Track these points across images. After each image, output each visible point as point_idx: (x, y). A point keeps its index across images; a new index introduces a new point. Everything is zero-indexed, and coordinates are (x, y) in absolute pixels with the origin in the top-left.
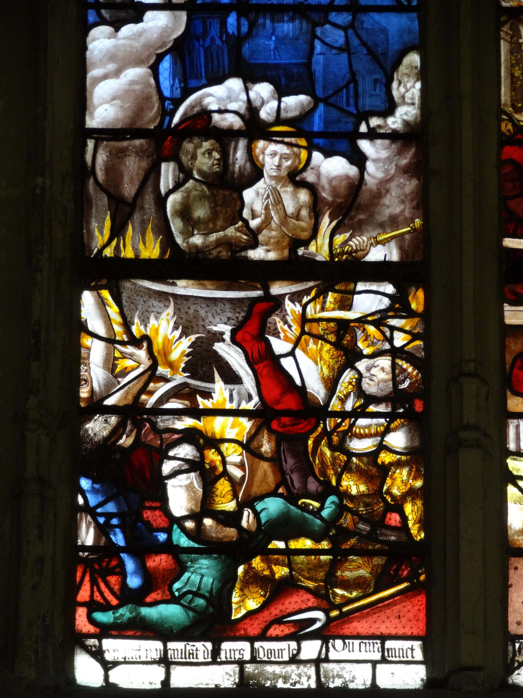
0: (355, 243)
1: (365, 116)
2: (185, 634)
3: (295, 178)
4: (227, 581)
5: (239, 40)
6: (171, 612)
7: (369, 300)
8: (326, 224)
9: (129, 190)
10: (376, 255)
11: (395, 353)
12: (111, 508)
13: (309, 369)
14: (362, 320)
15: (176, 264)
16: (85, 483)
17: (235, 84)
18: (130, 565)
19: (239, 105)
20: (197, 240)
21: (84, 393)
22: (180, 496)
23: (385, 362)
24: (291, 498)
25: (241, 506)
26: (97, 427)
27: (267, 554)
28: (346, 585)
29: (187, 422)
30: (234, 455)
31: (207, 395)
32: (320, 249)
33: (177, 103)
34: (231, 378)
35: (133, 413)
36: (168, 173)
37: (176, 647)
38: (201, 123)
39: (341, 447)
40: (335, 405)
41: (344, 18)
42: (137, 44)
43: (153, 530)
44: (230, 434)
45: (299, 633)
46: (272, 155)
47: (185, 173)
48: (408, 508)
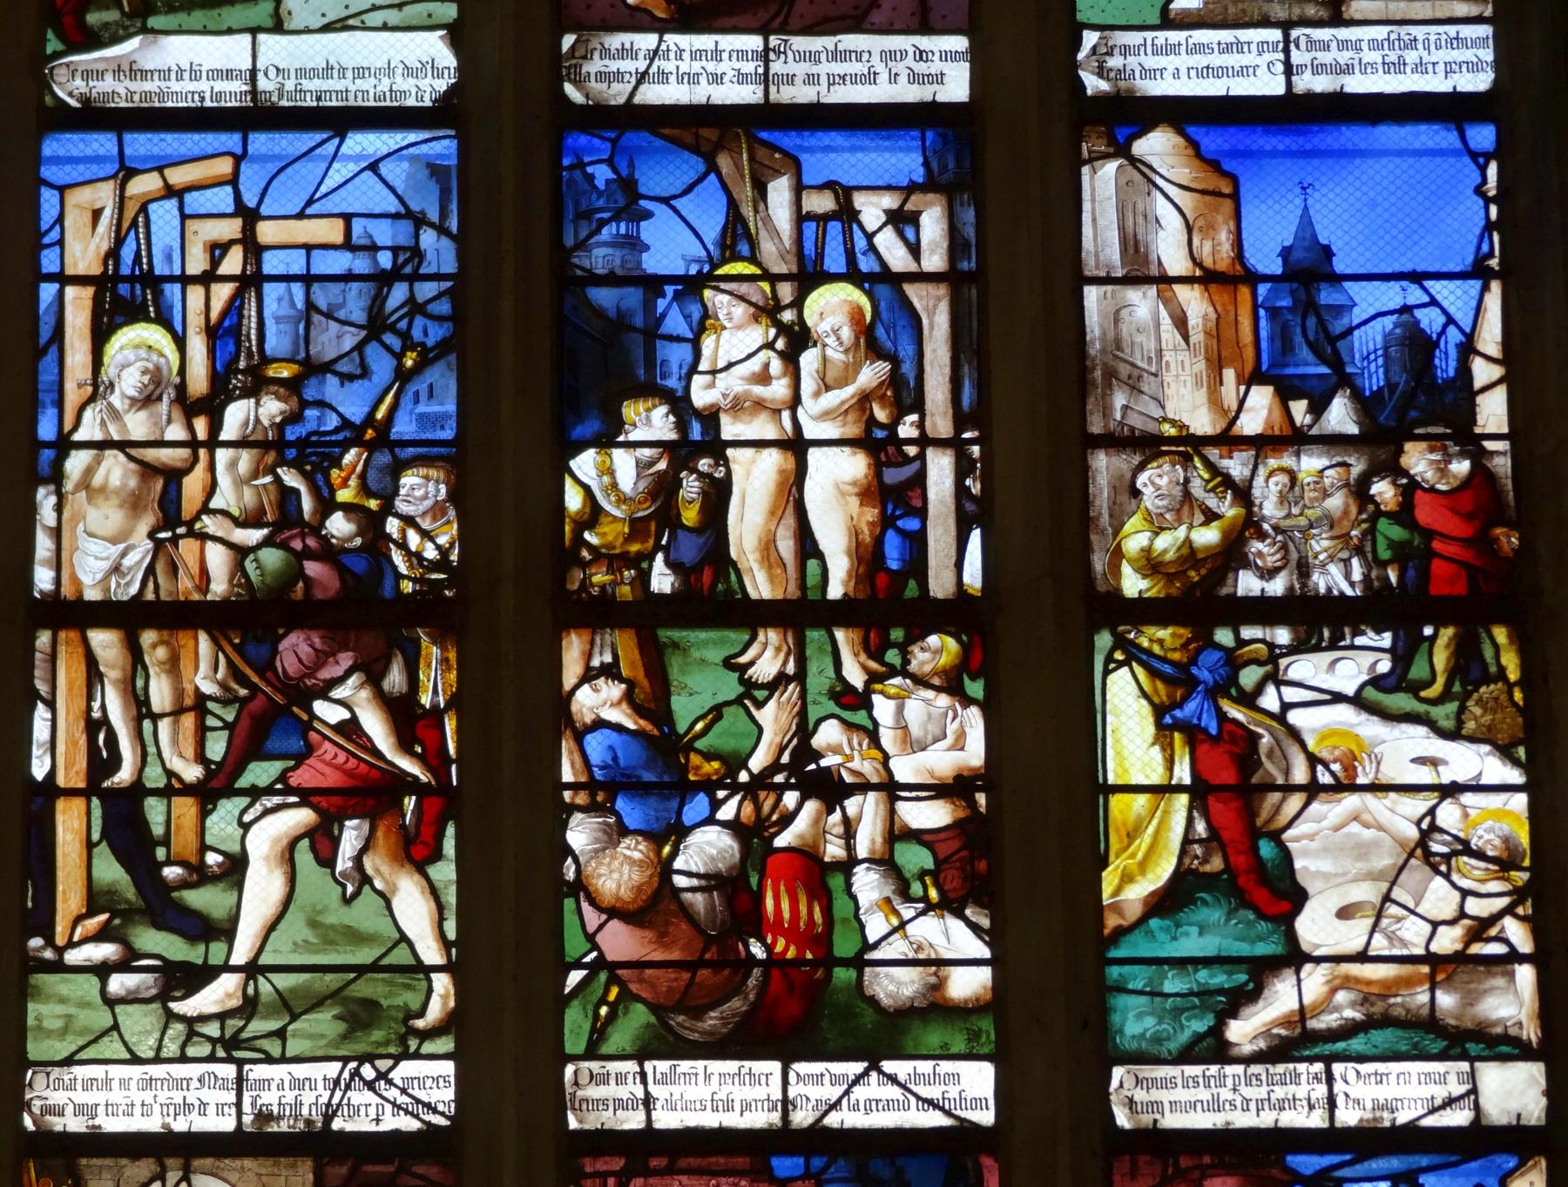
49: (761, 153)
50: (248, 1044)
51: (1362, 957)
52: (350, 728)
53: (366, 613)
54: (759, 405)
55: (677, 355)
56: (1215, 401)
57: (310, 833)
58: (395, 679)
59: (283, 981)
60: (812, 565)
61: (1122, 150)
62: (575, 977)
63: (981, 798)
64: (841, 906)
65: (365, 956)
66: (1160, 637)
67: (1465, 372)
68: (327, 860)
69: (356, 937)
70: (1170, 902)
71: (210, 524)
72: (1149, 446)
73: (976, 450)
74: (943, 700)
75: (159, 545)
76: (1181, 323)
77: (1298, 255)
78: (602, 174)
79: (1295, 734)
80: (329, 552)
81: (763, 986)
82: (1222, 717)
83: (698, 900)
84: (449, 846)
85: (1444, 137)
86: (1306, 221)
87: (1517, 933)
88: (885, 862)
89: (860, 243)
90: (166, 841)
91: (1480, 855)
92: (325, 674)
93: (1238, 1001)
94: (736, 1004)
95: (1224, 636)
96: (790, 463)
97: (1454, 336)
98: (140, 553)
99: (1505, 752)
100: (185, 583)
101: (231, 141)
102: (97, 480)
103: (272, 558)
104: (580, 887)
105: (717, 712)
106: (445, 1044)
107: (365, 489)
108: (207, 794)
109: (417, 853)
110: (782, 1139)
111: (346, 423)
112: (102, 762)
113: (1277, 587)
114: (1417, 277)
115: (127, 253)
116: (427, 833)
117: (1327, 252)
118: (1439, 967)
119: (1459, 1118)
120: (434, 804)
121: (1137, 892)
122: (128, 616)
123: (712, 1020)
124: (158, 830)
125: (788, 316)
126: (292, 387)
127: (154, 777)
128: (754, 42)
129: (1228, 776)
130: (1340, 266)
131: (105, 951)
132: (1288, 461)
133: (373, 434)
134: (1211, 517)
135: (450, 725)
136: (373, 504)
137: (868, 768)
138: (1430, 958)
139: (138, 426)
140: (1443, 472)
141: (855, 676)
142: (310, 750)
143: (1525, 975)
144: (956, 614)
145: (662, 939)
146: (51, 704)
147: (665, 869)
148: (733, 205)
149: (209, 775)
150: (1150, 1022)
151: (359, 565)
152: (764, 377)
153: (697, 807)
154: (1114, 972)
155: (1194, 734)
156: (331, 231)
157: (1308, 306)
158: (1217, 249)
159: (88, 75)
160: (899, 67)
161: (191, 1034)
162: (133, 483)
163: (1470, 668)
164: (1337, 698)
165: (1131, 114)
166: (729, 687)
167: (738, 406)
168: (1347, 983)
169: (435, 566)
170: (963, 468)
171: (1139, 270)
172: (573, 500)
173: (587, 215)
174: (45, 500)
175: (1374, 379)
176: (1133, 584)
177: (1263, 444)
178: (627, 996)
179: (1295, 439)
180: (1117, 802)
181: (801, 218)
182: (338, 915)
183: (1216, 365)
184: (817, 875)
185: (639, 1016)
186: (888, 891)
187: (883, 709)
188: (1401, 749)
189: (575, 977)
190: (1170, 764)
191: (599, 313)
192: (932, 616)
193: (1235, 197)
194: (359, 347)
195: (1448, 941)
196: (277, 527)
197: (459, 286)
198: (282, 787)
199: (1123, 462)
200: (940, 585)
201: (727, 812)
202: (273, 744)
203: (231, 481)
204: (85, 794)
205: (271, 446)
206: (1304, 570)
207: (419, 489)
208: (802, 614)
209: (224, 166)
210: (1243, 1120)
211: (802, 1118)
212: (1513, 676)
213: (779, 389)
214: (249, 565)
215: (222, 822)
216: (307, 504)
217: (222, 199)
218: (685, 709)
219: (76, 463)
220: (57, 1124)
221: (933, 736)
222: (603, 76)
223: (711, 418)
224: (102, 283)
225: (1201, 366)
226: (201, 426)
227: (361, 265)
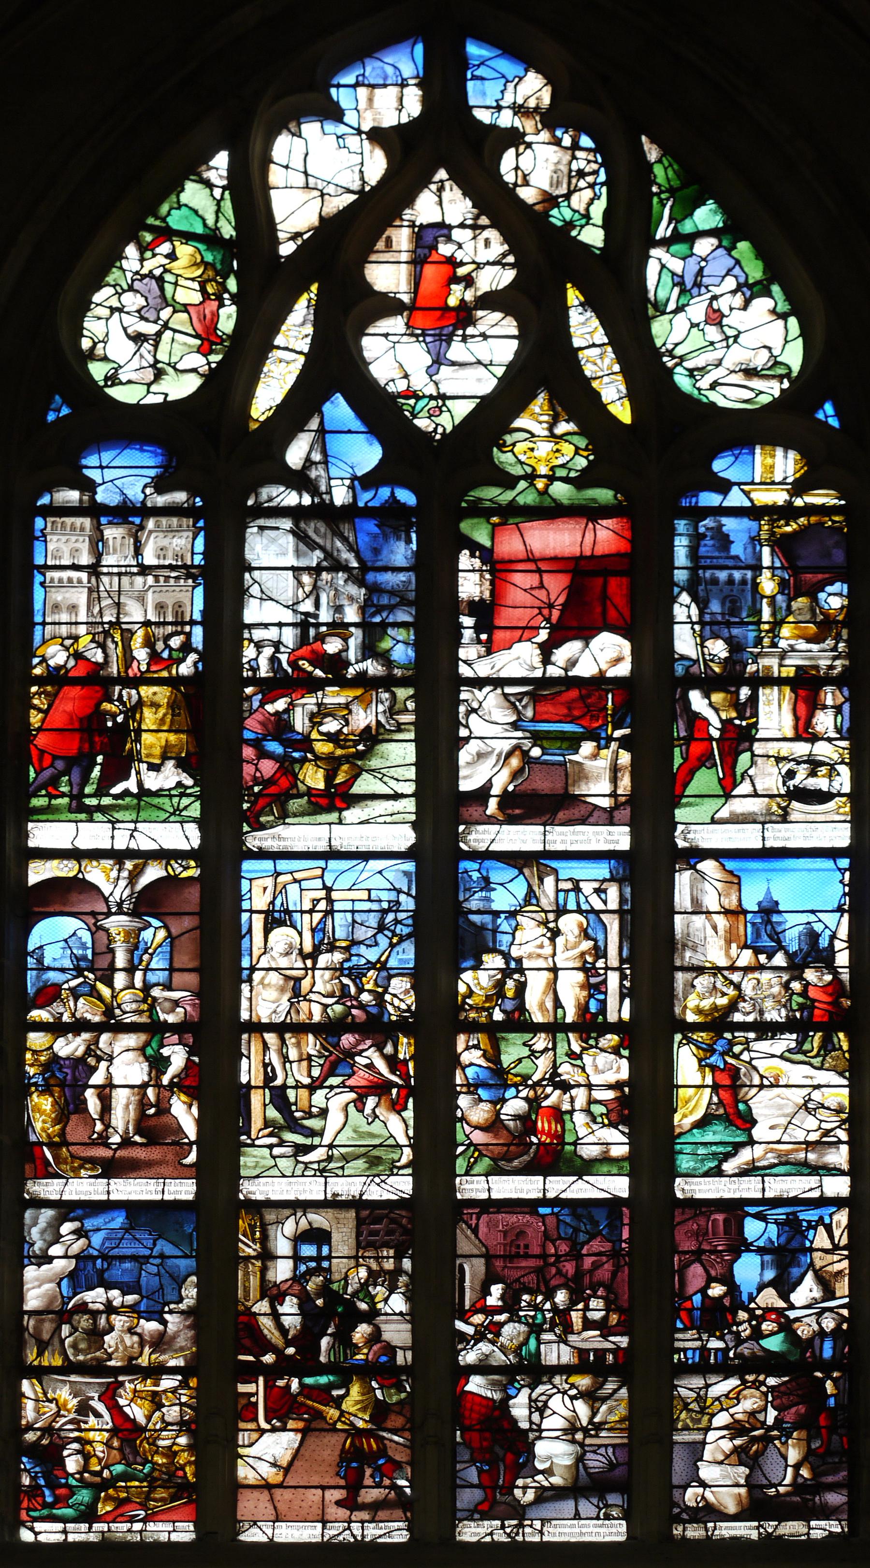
0: (162, 1358)
1: (168, 1304)
2: (74, 1520)
3: (131, 1331)
4: (96, 1500)
5: (103, 1271)
6: (68, 1512)
7: (168, 1383)
8: (147, 1350)
9: (46, 1336)
10: (172, 1363)
11: (181, 1405)
12: (37, 1469)
13: (137, 1412)
14: (165, 1391)
15: (69, 1368)
16: (25, 1459)
17: (101, 1290)
18: (47, 1492)
19: (104, 1300)
20: (81, 1358)
21: (24, 1422)
22: (72, 1464)
23: (177, 1408)
24: (128, 1465)
25: (103, 1469)
26: (30, 1437)
27: (116, 1488)
28: (155, 1500)
29: (76, 1434)
30: (99, 1448)
31: (86, 1423)
32: (144, 1361)
33: (70, 1299)
34: (98, 1415)
35: (48, 1430)
36: (65, 1329)
37: (70, 1526)
38: (83, 1308)
39: (154, 1444)
40: (150, 1426)
41: (157, 1261)
42: (50, 1274)
43: (58, 1478)
44: (98, 1438)
45: (132, 1520)
46: (119, 1321)
47: (75, 1329)
48: (187, 1469)
49: (542, 868)
50: (329, 1171)
51: (779, 1142)
52: (370, 1066)
53: (378, 1028)
54: (539, 956)
55: (505, 939)
56: (728, 954)
57: (354, 1101)
58: (389, 1049)
59: (343, 1150)
60: (560, 1011)
61: (693, 867)
62: (460, 1149)
63: (627, 1090)
64: (569, 1125)
65: (377, 1142)
66: (701, 1036)
67: (831, 944)
68: (361, 1110)
69: (372, 1135)
70: (702, 1124)
71: (312, 996)
72: (700, 970)
73: (628, 972)
74: (613, 1056)
75: (292, 1004)
76: (715, 928)
77: (764, 904)
78: (475, 875)
79: (755, 1068)
80: (362, 1006)
81: (536, 1153)
82: (725, 1062)
83: (511, 1123)
84: (410, 1104)
85: (829, 864)
86: (768, 892)
87: (843, 1135)
88: (587, 1111)
89: (582, 899)
90: (296, 1104)
91: (828, 1108)
92: (360, 1047)
93: (727, 1157)
94: (526, 1158)
95: (728, 1035)
96: (551, 976)
97: (828, 933)
98: (285, 1005)
99: (841, 1074)
100: (303, 1017)
101: (321, 863)
102: (266, 982)
103: (339, 1008)
104: (463, 1119)
105: (520, 1061)
106: (409, 1171)
107: (376, 984)
108: (312, 1088)
109: (397, 1107)
110: (544, 1202)
111: (369, 962)
112: (269, 1078)
113: (750, 1018)
114: (813, 912)
115: (278, 902)
116: (401, 1101)
117: (777, 903)
118: (809, 1145)
119: (816, 1194)
120: (404, 1092)
121: (687, 1122)
122: (280, 1029)
123: (516, 1163)
124: (292, 1100)
125: (552, 925)
126: (347, 949)
127: (291, 1082)
128: (541, 828)
129: (727, 1082)
130: (781, 908)
131: (274, 1140)
132: (756, 975)
133: (381, 966)
134: (724, 994)
135: (411, 1065)
136: (380, 990)
137: (582, 1080)
138: (807, 1143)
139: (284, 962)
140: (821, 979)
141: (576, 1048)
142: (354, 1073)
143: (844, 1149)
144: (618, 1027)
145: (496, 1136)
146: (249, 1058)
147: (498, 1113)
148: (530, 886)
149: (313, 1082)
150: (692, 1164)
151: (374, 1011)
152: (541, 946)
153: (511, 1092)
154: (678, 1147)
155: (714, 1068)
156: (364, 895)
157: (769, 922)
158: (731, 902)
159: (260, 839)
160: (601, 838)
161: (306, 1168)
162: (281, 982)
163: (827, 1046)
164: (773, 1056)
165: (698, 854)
166: (526, 1052)
167: (530, 956)
168: (772, 1151)
169: (405, 1011)
170: (623, 977)
171: (698, 909)
172: (462, 988)
173: (469, 889)
174: (245, 988)
175: (794, 947)
176: (691, 1017)
177: (746, 970)
178: (481, 1155)
179: (761, 968)
180: (681, 1091)
181: (558, 891)
182: (366, 1128)
183: (729, 942)
184: (557, 1114)
185: (486, 1161)
186: (588, 1120)
187: (587, 1059)
188: (797, 1073)
189: (460, 1149)
190: (704, 1077)
191: (473, 924)
192: (607, 1028)
193: (739, 884)
194: (374, 936)
195: (814, 1137)
196: (341, 997)
197: (416, 915)
198: (343, 1085)
199: (689, 976)
200: (612, 1017)
201: (523, 1094)
202: (339, 1070)
203: (323, 981)
204: (263, 1088)
205: (338, 970)
206: (761, 1012)
207: (399, 985)
208: (554, 1028)
209: (319, 872)
210: (727, 1196)
211: (551, 1195)
212: (845, 1046)
213: (548, 950)
214: (329, 1010)
215: (319, 1098)
216: (353, 990)
217: (318, 883)
218: (506, 1060)
219: (257, 976)
220: (253, 1197)
221: (608, 1068)
222: (475, 840)
223: (519, 961)
224: (267, 913)
225: (722, 942)
226: (309, 963)
227: (375, 906)
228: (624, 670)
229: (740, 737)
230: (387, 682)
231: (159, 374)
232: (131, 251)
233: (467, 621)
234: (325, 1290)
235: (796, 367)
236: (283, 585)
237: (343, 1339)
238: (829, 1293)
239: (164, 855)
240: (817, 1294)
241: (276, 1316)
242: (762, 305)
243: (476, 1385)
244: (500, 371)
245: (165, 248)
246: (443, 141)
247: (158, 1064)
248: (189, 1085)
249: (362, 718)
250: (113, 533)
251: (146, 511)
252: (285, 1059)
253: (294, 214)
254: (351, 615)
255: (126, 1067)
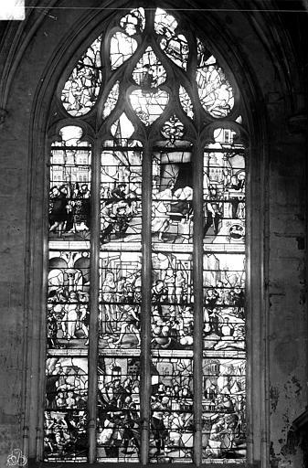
52: (131, 315)
177: (221, 288)
215: (119, 324)
228: (190, 198)
229: (219, 217)
230: (136, 199)
231: (81, 107)
232: (75, 70)
233: (154, 182)
234: (119, 385)
235: (232, 107)
236: (112, 171)
237: (123, 400)
238: (240, 389)
239: (83, 251)
240: (237, 389)
241: (107, 393)
242: (224, 87)
243: (156, 415)
244: (164, 107)
245: (83, 70)
246: (147, 36)
247: (79, 314)
248: (86, 321)
249: (129, 210)
250: (69, 154)
251: (77, 148)
252: (111, 313)
253: (116, 61)
254: (127, 180)
255: (72, 316)
